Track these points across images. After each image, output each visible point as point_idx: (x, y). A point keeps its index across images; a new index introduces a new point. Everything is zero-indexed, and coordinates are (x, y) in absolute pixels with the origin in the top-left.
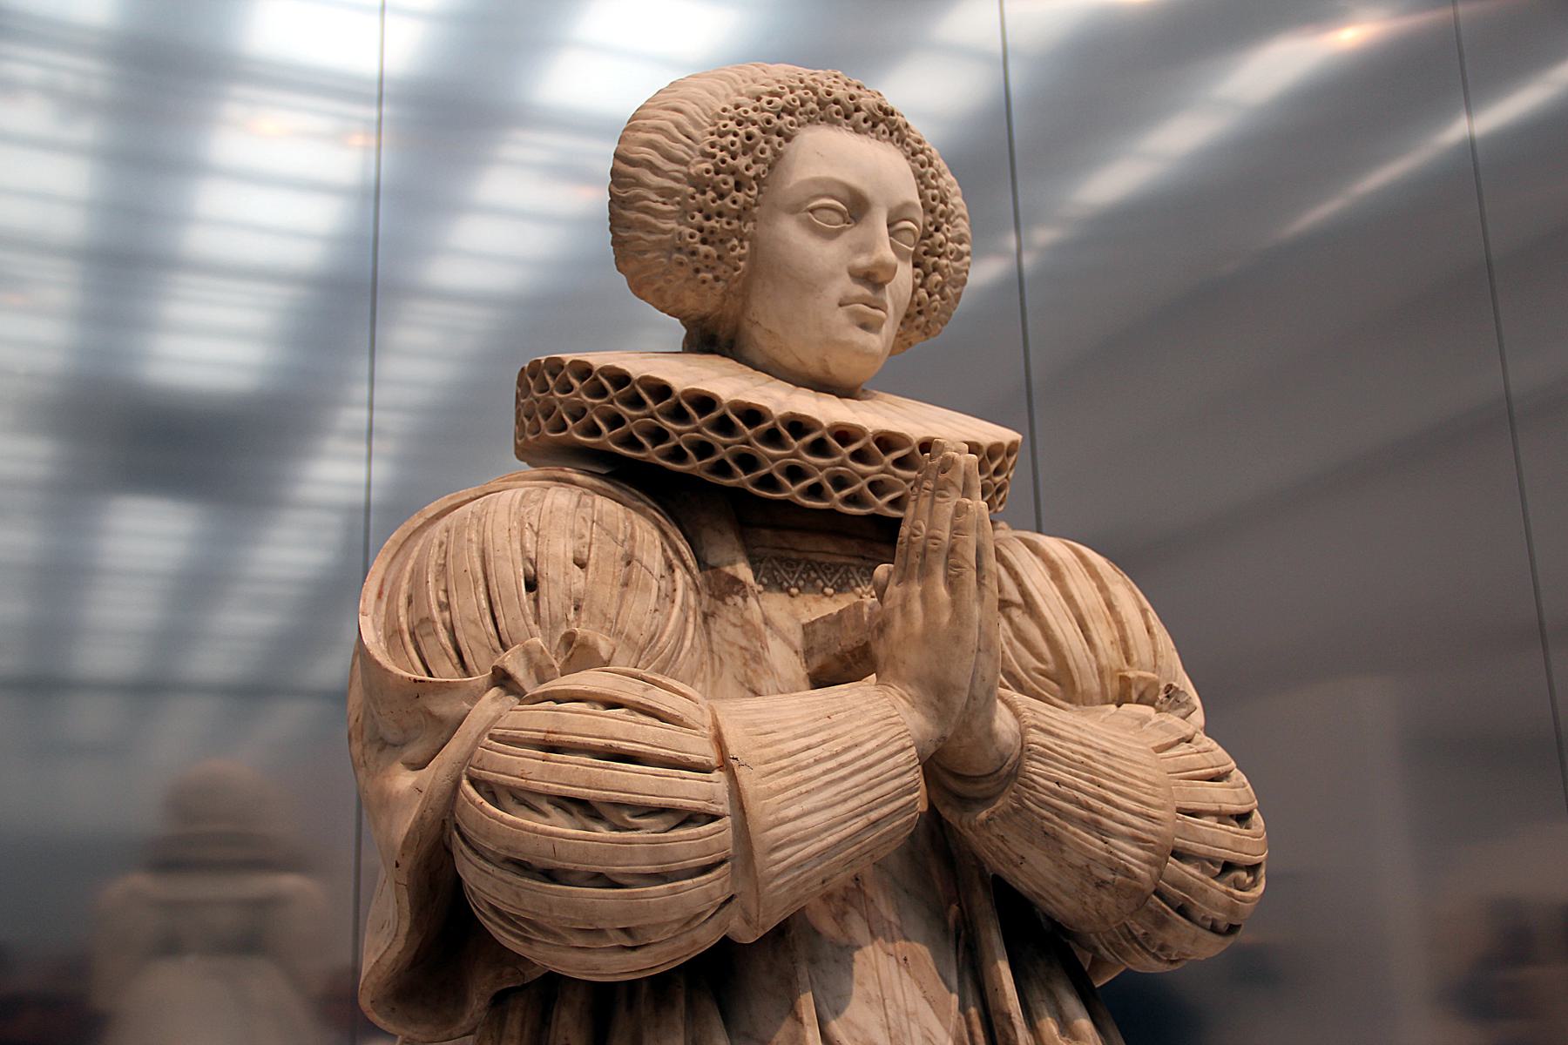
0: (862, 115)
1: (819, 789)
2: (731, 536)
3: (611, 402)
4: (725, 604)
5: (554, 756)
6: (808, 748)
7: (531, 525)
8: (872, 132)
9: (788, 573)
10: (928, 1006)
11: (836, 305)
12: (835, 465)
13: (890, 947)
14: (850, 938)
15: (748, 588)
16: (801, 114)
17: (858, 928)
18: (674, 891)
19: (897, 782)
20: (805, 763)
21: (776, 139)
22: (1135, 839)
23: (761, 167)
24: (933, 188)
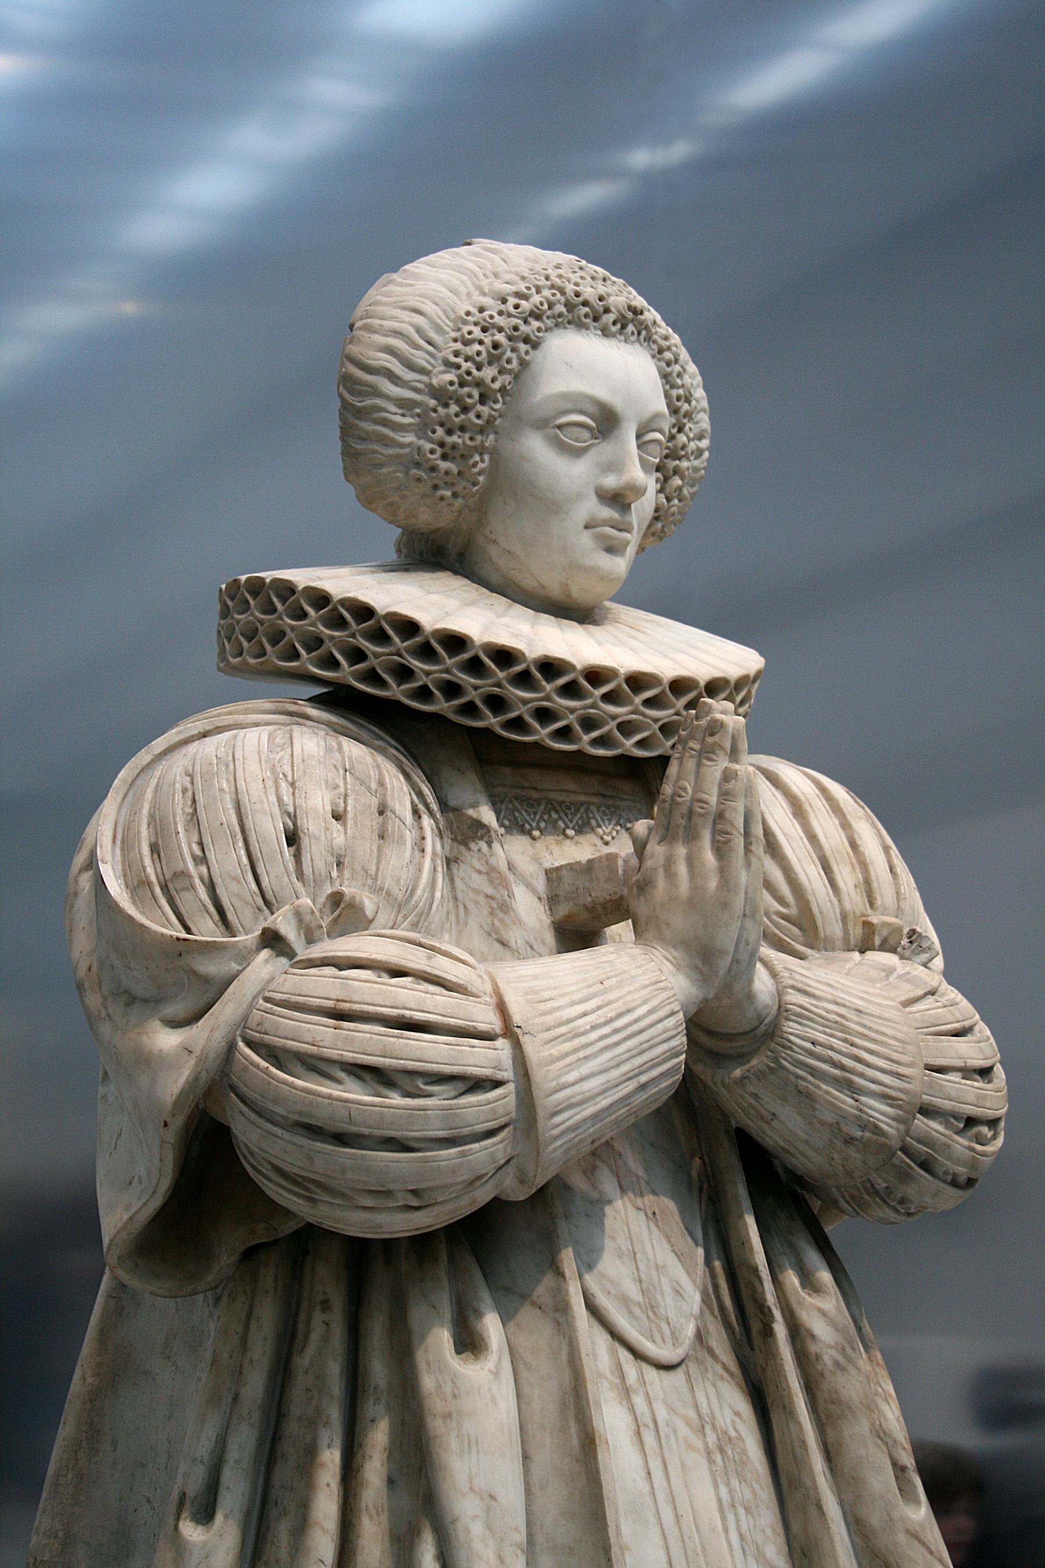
0: (610, 317)
1: (595, 1055)
2: (472, 776)
3: (353, 636)
4: (469, 849)
5: (345, 1024)
6: (585, 1014)
7: (285, 775)
8: (620, 334)
9: (529, 813)
10: (676, 1260)
11: (581, 527)
12: (585, 707)
13: (639, 1201)
14: (600, 1192)
15: (493, 833)
16: (548, 318)
17: (608, 1184)
18: (463, 1154)
19: (665, 1046)
20: (582, 1030)
21: (523, 347)
22: (885, 1097)
23: (507, 378)
24: (678, 388)
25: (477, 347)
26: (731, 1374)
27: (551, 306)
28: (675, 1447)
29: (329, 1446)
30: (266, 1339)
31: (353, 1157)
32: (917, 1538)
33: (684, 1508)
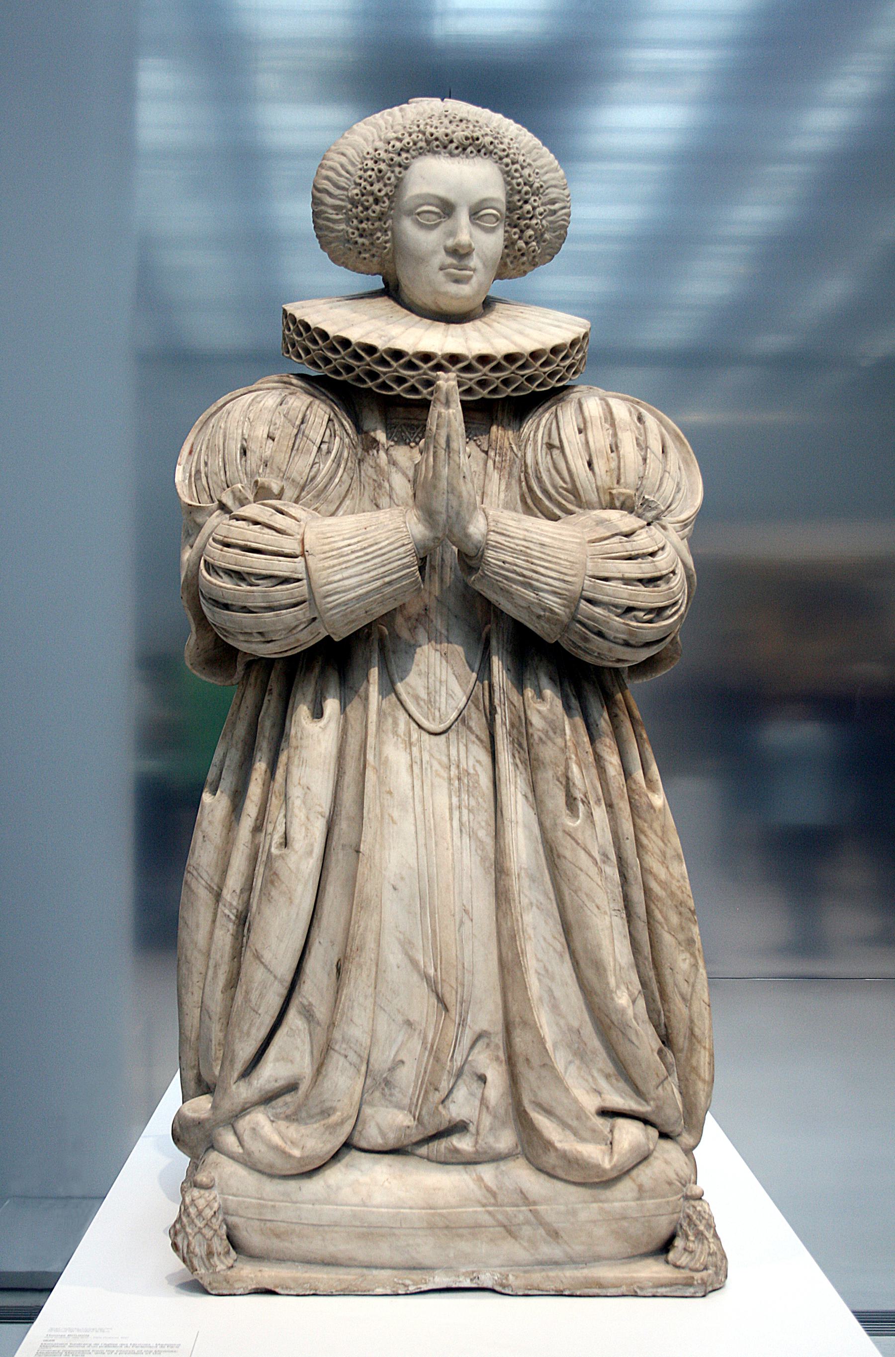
0: (454, 145)
1: (353, 566)
2: (377, 413)
3: (304, 340)
4: (369, 454)
5: (225, 549)
6: (349, 545)
7: (249, 419)
8: (463, 154)
9: (410, 433)
10: (455, 678)
11: (437, 270)
12: (419, 375)
13: (438, 647)
14: (416, 641)
15: (380, 445)
16: (414, 150)
17: (422, 635)
18: (277, 615)
19: (399, 563)
20: (345, 553)
21: (397, 169)
22: (554, 593)
23: (389, 189)
24: (517, 178)
25: (369, 173)
26: (481, 741)
27: (415, 144)
28: (429, 774)
29: (260, 761)
30: (247, 707)
31: (228, 615)
32: (570, 835)
33: (429, 805)
